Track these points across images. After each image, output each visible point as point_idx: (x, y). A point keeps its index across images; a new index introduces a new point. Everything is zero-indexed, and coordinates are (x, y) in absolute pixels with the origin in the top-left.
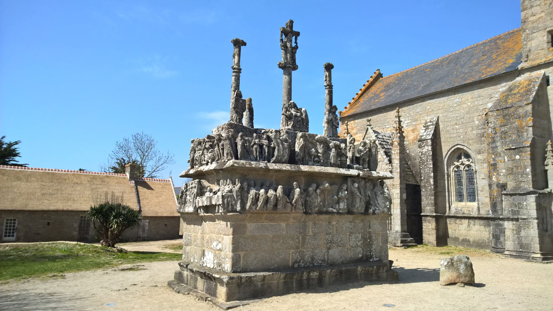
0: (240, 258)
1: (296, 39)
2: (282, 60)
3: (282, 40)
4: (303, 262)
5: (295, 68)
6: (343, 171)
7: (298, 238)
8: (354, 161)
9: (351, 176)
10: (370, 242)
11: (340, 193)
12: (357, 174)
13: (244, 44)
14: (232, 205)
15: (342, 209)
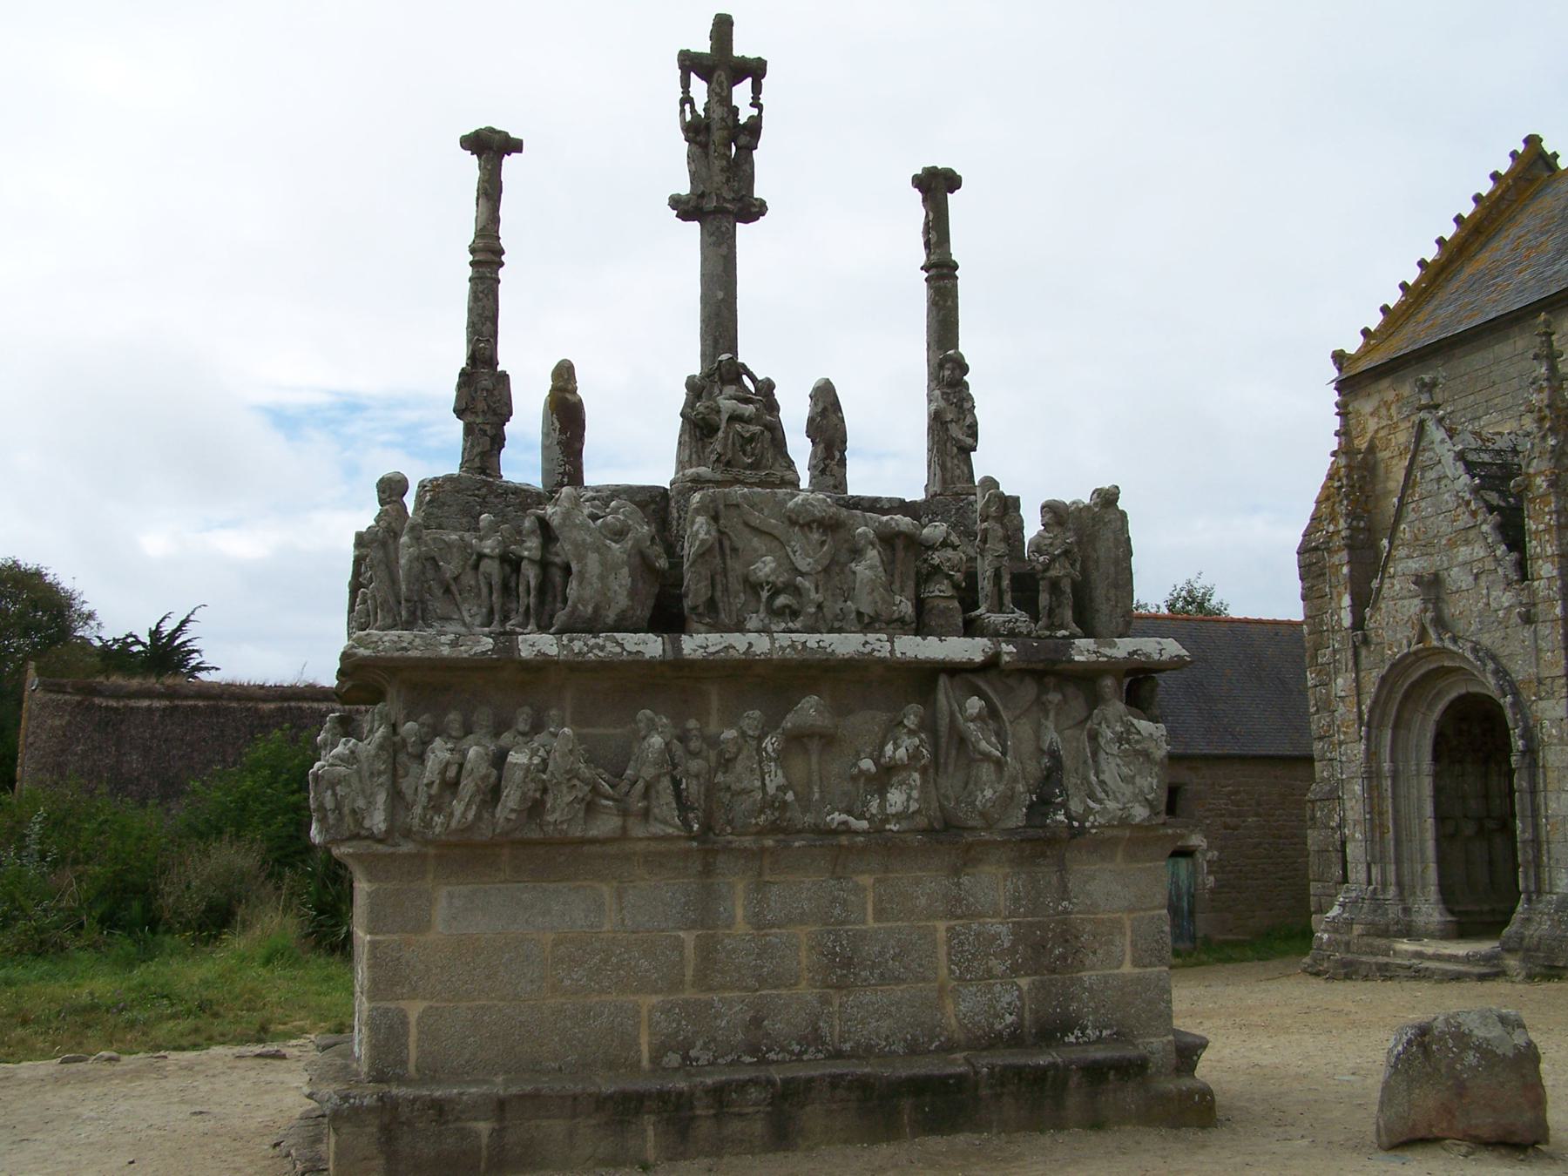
0: (404, 1022)
1: (757, 89)
2: (684, 188)
3: (687, 99)
4: (705, 1047)
5: (753, 210)
6: (912, 647)
7: (679, 945)
8: (1007, 598)
9: (954, 670)
10: (1063, 957)
11: (889, 748)
12: (979, 658)
13: (516, 146)
14: (354, 812)
15: (898, 817)
